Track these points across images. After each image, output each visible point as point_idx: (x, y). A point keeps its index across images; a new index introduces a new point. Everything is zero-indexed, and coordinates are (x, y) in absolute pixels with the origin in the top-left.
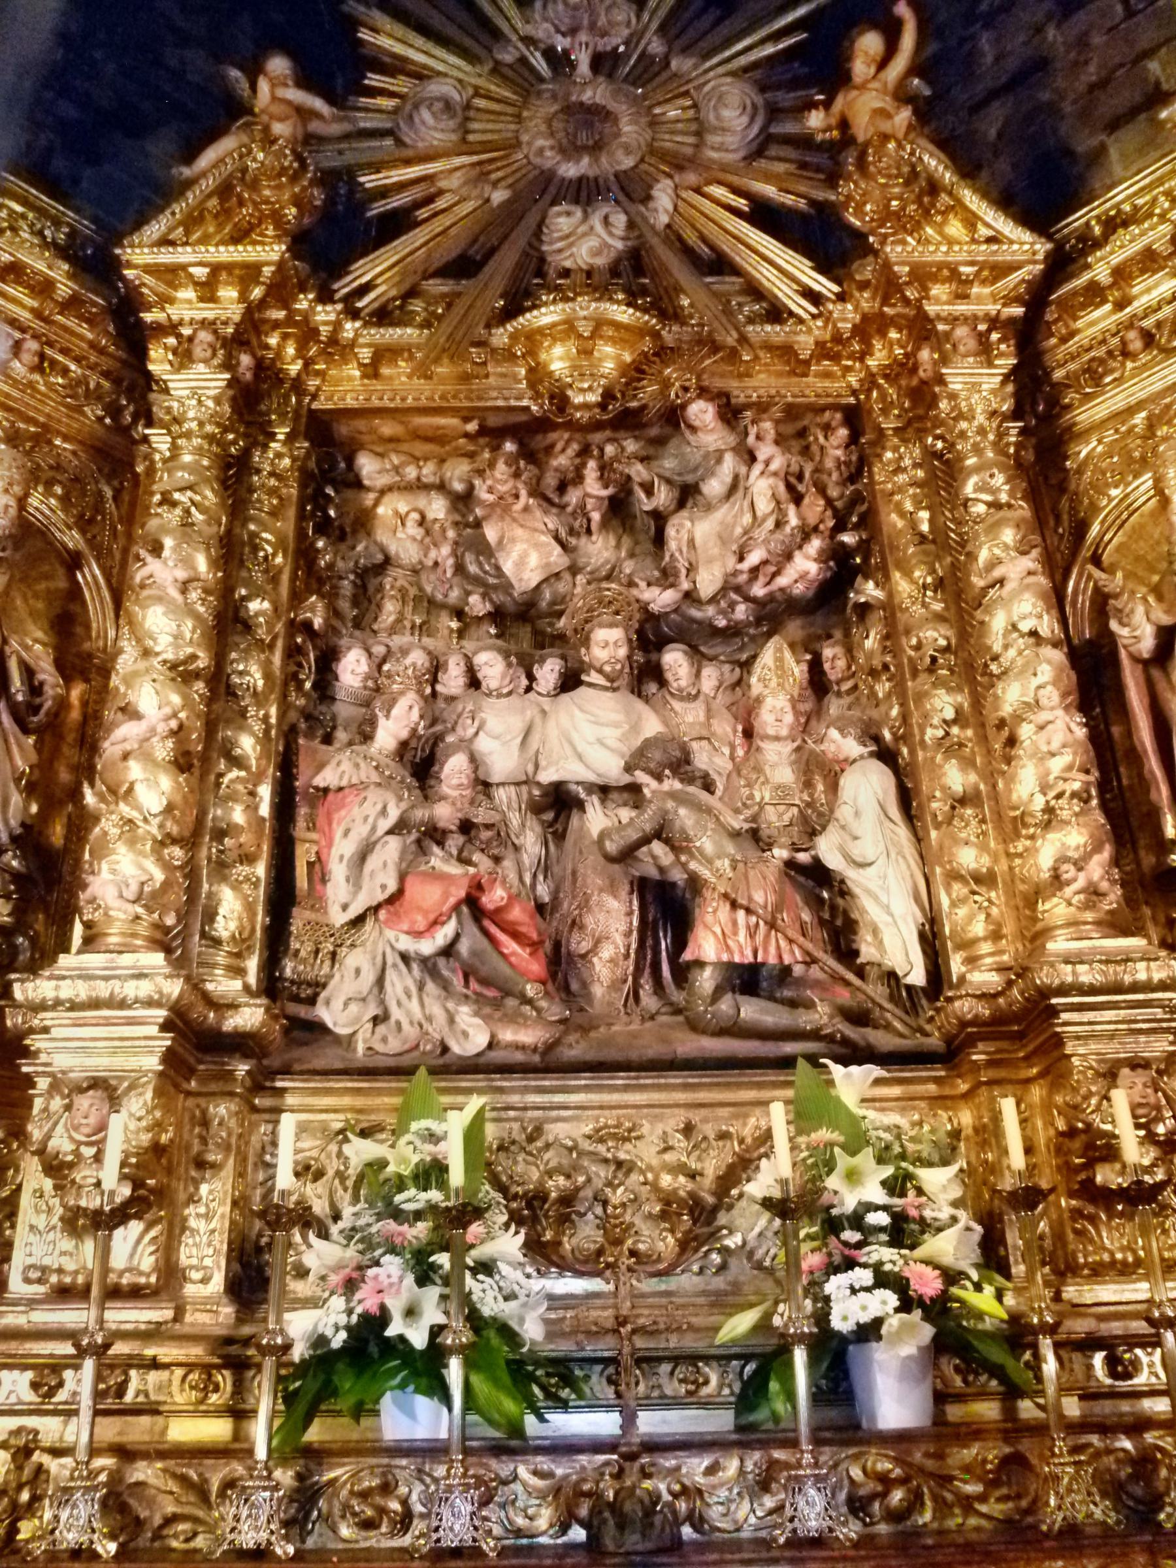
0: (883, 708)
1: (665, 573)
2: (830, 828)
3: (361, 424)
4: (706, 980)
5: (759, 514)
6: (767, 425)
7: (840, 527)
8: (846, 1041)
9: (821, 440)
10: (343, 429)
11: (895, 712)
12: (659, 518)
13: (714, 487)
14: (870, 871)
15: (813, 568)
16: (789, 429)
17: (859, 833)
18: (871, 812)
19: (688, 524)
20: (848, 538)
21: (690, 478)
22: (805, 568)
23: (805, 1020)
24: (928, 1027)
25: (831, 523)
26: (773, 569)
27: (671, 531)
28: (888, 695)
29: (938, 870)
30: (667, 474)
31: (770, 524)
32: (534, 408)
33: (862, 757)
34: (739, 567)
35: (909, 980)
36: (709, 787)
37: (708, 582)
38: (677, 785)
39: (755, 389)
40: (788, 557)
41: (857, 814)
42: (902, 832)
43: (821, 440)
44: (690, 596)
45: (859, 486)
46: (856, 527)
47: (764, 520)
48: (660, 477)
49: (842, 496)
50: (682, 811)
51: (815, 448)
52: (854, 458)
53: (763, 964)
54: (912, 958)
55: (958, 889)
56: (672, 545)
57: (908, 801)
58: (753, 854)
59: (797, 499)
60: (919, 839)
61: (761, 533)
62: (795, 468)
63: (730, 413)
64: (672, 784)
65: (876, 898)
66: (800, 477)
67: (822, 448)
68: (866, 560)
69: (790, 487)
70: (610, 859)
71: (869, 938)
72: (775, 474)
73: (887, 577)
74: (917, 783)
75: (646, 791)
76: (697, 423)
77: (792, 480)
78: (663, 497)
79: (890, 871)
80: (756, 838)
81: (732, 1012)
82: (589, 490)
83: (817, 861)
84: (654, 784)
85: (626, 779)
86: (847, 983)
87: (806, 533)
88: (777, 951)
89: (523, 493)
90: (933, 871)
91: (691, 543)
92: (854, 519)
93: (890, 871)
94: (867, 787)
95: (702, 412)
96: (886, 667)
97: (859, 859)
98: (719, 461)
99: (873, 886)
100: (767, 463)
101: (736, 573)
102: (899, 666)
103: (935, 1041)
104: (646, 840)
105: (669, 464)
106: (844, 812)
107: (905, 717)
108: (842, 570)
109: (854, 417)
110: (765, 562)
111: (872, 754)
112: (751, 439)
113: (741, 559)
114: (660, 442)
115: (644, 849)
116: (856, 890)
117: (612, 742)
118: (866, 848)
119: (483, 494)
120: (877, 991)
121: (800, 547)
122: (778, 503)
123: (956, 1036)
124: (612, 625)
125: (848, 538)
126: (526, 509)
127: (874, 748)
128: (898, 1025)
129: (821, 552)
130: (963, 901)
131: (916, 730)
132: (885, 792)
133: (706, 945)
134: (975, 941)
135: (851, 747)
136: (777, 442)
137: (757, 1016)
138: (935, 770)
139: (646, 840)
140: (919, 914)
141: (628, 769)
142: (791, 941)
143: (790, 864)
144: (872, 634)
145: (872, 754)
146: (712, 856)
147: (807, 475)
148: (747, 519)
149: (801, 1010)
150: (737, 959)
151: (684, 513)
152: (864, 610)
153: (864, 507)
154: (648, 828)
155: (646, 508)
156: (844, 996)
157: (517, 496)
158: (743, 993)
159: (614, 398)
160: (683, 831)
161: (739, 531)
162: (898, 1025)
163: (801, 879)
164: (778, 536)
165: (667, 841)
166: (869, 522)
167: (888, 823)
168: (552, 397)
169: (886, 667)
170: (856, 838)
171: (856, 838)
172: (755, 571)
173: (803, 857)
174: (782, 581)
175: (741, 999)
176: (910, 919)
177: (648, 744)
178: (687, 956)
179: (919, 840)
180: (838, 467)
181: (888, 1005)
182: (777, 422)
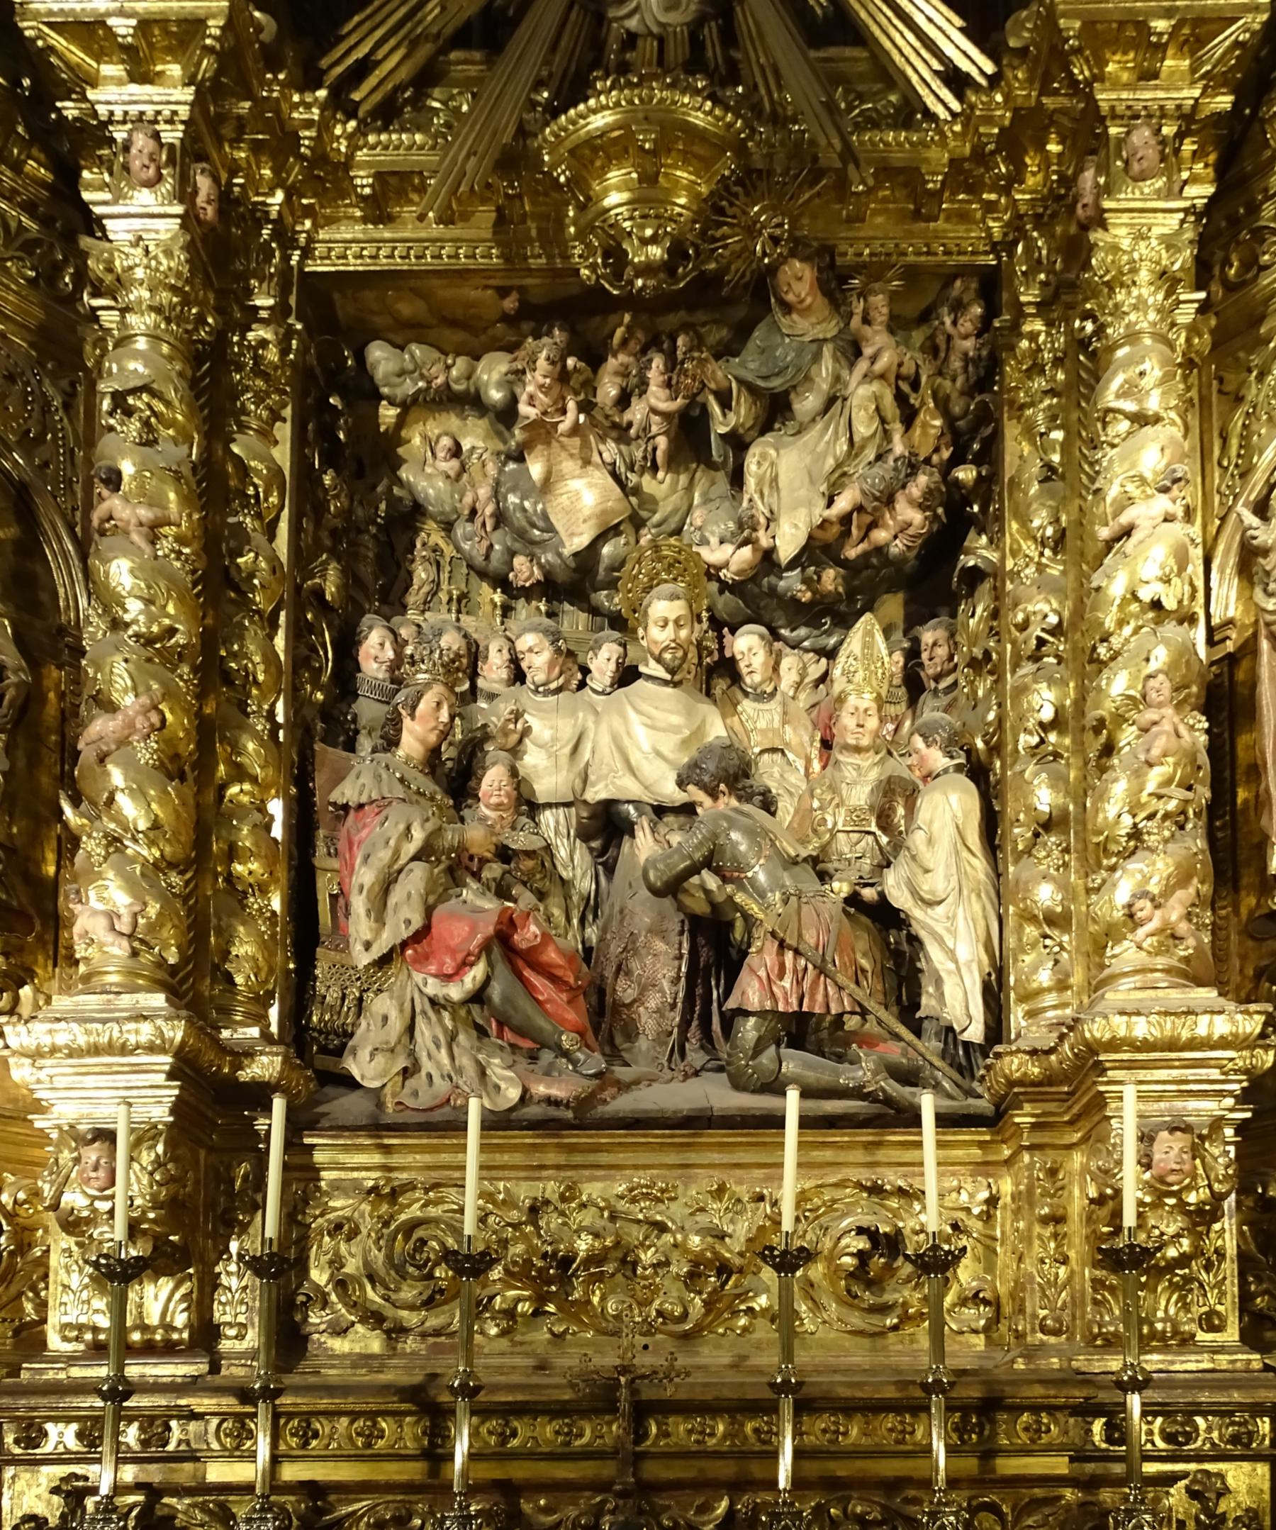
0: (979, 708)
1: (741, 526)
2: (901, 858)
3: (369, 296)
4: (749, 1030)
5: (856, 439)
6: (879, 302)
7: (957, 459)
8: (888, 1101)
9: (948, 321)
10: (344, 308)
11: (991, 716)
12: (738, 443)
13: (807, 403)
14: (940, 910)
15: (917, 517)
16: (911, 309)
17: (931, 866)
18: (946, 837)
19: (772, 452)
20: (966, 474)
21: (776, 383)
22: (910, 516)
23: (848, 1076)
24: (980, 1090)
25: (946, 454)
26: (868, 519)
27: (752, 465)
28: (988, 693)
29: (1011, 909)
30: (749, 377)
31: (870, 454)
32: (585, 272)
33: (946, 771)
34: (827, 513)
35: (966, 1036)
36: (768, 805)
37: (788, 540)
38: (734, 802)
39: (868, 241)
40: (888, 500)
41: (930, 841)
42: (979, 866)
43: (948, 321)
44: (768, 557)
45: (987, 397)
46: (977, 462)
47: (863, 448)
48: (741, 382)
49: (966, 412)
50: (735, 836)
51: (941, 340)
52: (984, 353)
53: (811, 1014)
54: (973, 1011)
55: (1031, 931)
56: (751, 483)
57: (991, 824)
58: (811, 884)
59: (909, 417)
60: (998, 874)
61: (858, 468)
62: (909, 369)
63: (836, 284)
64: (728, 803)
65: (940, 941)
66: (915, 385)
67: (949, 338)
68: (984, 509)
69: (900, 398)
70: (656, 892)
71: (931, 990)
72: (882, 376)
73: (1002, 530)
74: (1004, 805)
75: (699, 810)
76: (790, 298)
77: (905, 387)
78: (743, 413)
79: (960, 912)
80: (820, 868)
81: (774, 1066)
82: (653, 401)
83: (882, 895)
84: (707, 801)
85: (679, 797)
86: (898, 1037)
87: (912, 466)
88: (828, 999)
89: (571, 405)
90: (1007, 910)
91: (775, 480)
92: (976, 446)
93: (960, 912)
94: (949, 808)
95: (799, 280)
96: (987, 654)
97: (926, 896)
98: (817, 357)
99: (939, 929)
100: (874, 359)
101: (825, 523)
102: (1001, 655)
103: (983, 1105)
104: (694, 870)
105: (749, 364)
106: (918, 840)
107: (1000, 720)
108: (958, 516)
109: (991, 286)
110: (859, 508)
111: (959, 768)
112: (856, 321)
113: (830, 503)
114: (743, 332)
115: (695, 880)
116: (923, 934)
117: (666, 751)
118: (935, 883)
119: (524, 409)
120: (931, 1046)
121: (904, 487)
122: (883, 421)
123: (1004, 1097)
124: (674, 597)
125: (966, 474)
126: (576, 430)
127: (962, 760)
128: (947, 1085)
129: (929, 493)
130: (1034, 945)
131: (1009, 738)
132: (966, 816)
133: (750, 992)
134: (1040, 991)
135: (937, 759)
136: (891, 331)
137: (798, 1071)
138: (1025, 787)
139: (694, 870)
140: (985, 958)
141: (681, 783)
142: (841, 988)
143: (853, 900)
144: (979, 610)
145: (959, 768)
146: (763, 892)
147: (924, 379)
148: (842, 447)
149: (847, 1065)
150: (781, 1008)
151: (769, 438)
152: (975, 576)
153: (988, 431)
154: (698, 856)
155: (722, 430)
156: (894, 1052)
157: (564, 411)
158: (788, 1046)
159: (686, 257)
160: (735, 859)
161: (830, 462)
162: (947, 1085)
163: (864, 919)
164: (878, 470)
165: (717, 871)
166: (990, 455)
167: (965, 854)
168: (606, 256)
169: (987, 654)
170: (927, 871)
171: (927, 871)
172: (846, 519)
173: (868, 894)
174: (880, 536)
175: (784, 1051)
176: (975, 967)
177: (708, 750)
178: (731, 1004)
179: (999, 876)
180: (965, 368)
181: (938, 1063)
182: (893, 297)
